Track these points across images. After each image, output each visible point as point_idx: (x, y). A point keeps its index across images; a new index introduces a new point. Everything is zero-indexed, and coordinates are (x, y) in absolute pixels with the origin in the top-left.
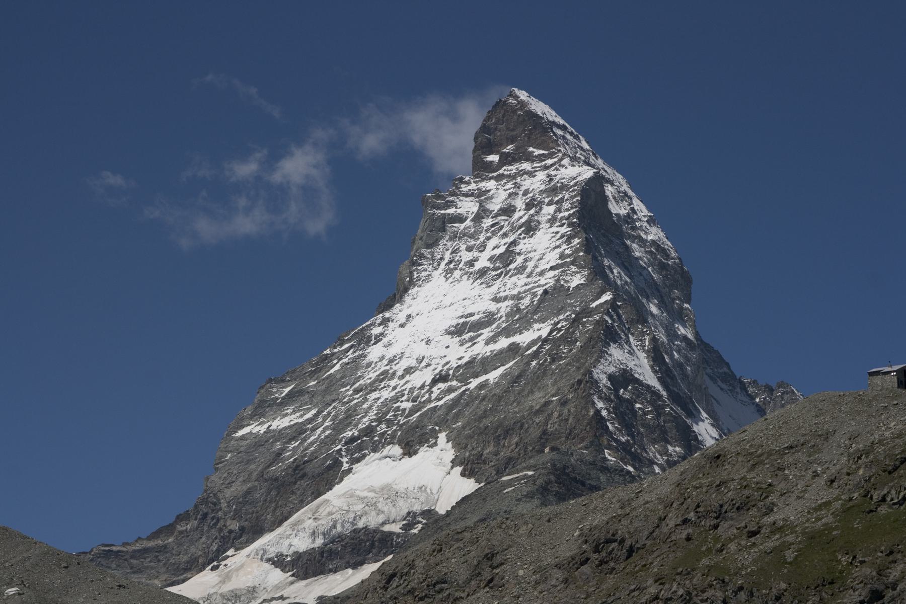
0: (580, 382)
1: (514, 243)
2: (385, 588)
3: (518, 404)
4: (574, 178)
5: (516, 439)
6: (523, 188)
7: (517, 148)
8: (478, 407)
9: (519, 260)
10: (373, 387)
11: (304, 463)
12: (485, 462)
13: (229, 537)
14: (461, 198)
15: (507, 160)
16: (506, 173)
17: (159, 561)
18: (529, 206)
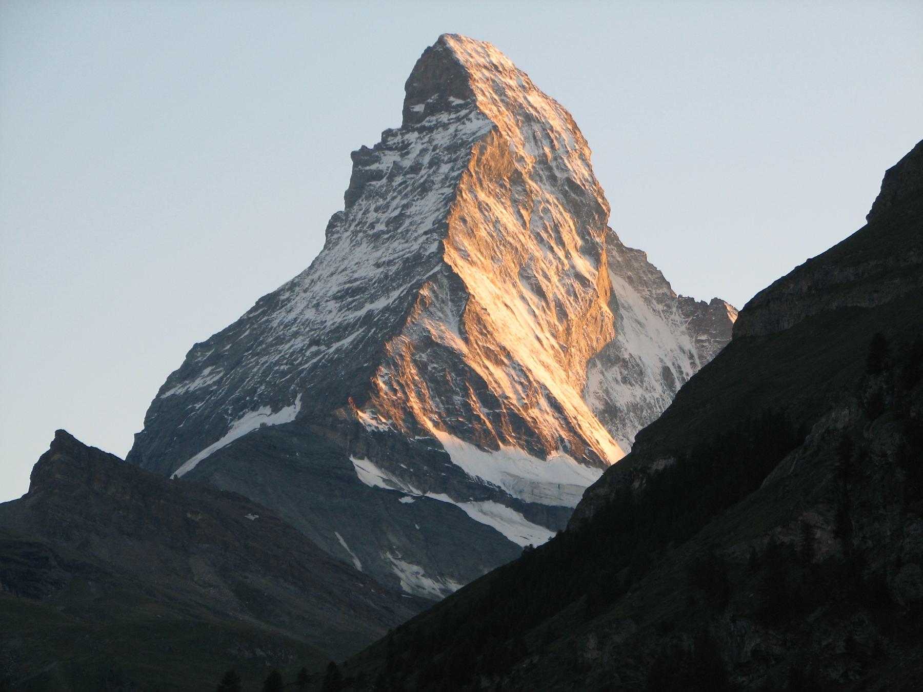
1: (406, 206)
4: (474, 134)
6: (434, 143)
9: (407, 222)
10: (266, 352)
14: (386, 152)
15: (432, 110)
16: (427, 124)
18: (430, 167)
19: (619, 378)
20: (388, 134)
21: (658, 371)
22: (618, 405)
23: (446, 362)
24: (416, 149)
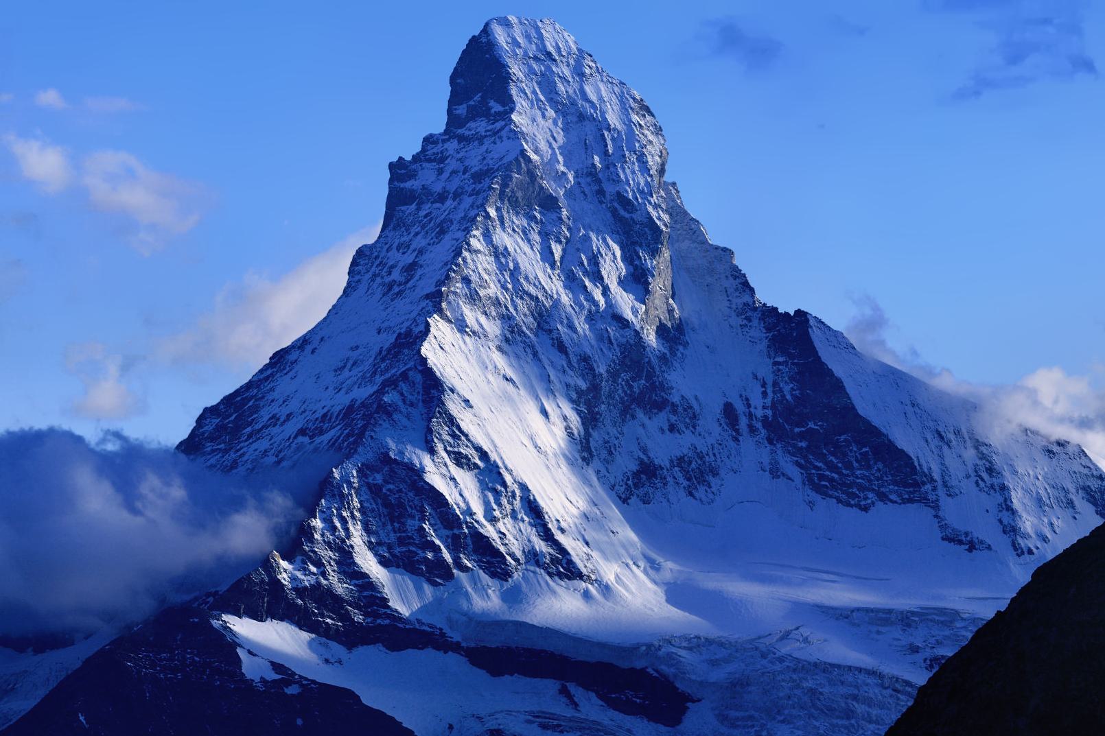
4: (501, 159)
7: (484, 101)
14: (425, 165)
15: (474, 114)
19: (666, 427)
20: (429, 140)
21: (718, 409)
22: (656, 462)
23: (404, 481)
24: (452, 164)
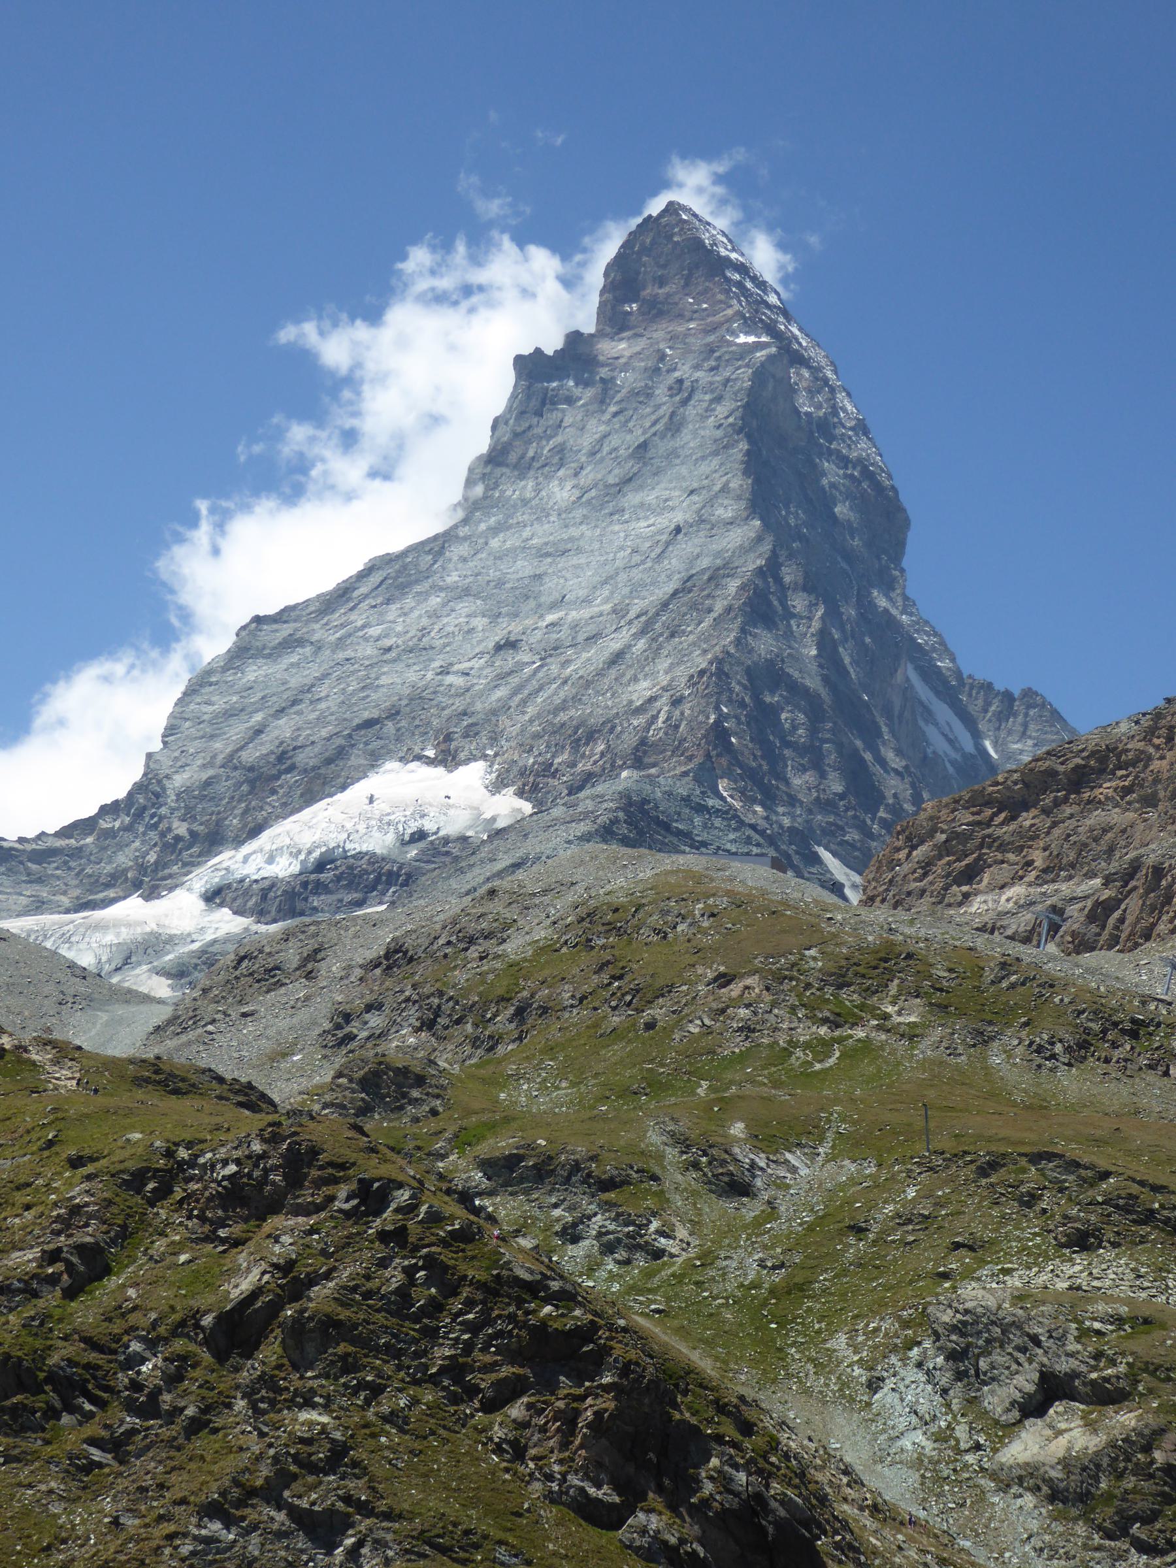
0: (702, 673)
2: (236, 968)
3: (613, 695)
5: (601, 747)
8: (555, 693)
11: (295, 749)
12: (554, 775)
13: (175, 845)
17: (70, 868)
